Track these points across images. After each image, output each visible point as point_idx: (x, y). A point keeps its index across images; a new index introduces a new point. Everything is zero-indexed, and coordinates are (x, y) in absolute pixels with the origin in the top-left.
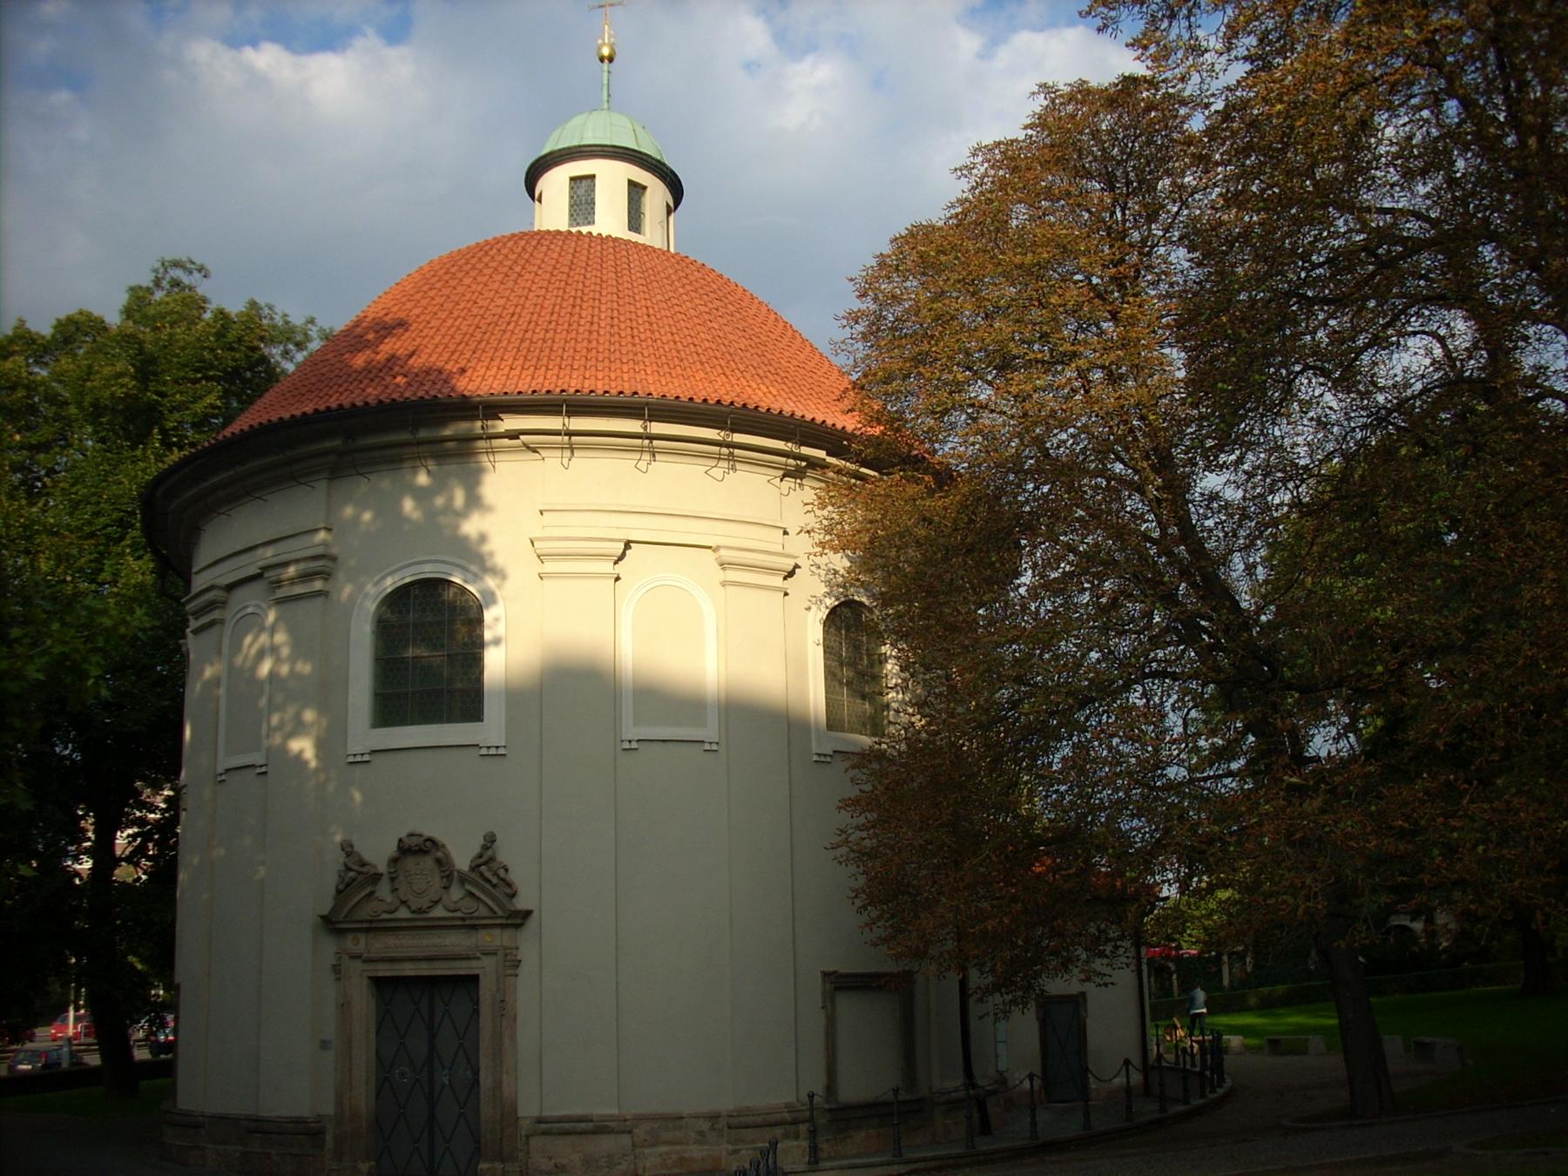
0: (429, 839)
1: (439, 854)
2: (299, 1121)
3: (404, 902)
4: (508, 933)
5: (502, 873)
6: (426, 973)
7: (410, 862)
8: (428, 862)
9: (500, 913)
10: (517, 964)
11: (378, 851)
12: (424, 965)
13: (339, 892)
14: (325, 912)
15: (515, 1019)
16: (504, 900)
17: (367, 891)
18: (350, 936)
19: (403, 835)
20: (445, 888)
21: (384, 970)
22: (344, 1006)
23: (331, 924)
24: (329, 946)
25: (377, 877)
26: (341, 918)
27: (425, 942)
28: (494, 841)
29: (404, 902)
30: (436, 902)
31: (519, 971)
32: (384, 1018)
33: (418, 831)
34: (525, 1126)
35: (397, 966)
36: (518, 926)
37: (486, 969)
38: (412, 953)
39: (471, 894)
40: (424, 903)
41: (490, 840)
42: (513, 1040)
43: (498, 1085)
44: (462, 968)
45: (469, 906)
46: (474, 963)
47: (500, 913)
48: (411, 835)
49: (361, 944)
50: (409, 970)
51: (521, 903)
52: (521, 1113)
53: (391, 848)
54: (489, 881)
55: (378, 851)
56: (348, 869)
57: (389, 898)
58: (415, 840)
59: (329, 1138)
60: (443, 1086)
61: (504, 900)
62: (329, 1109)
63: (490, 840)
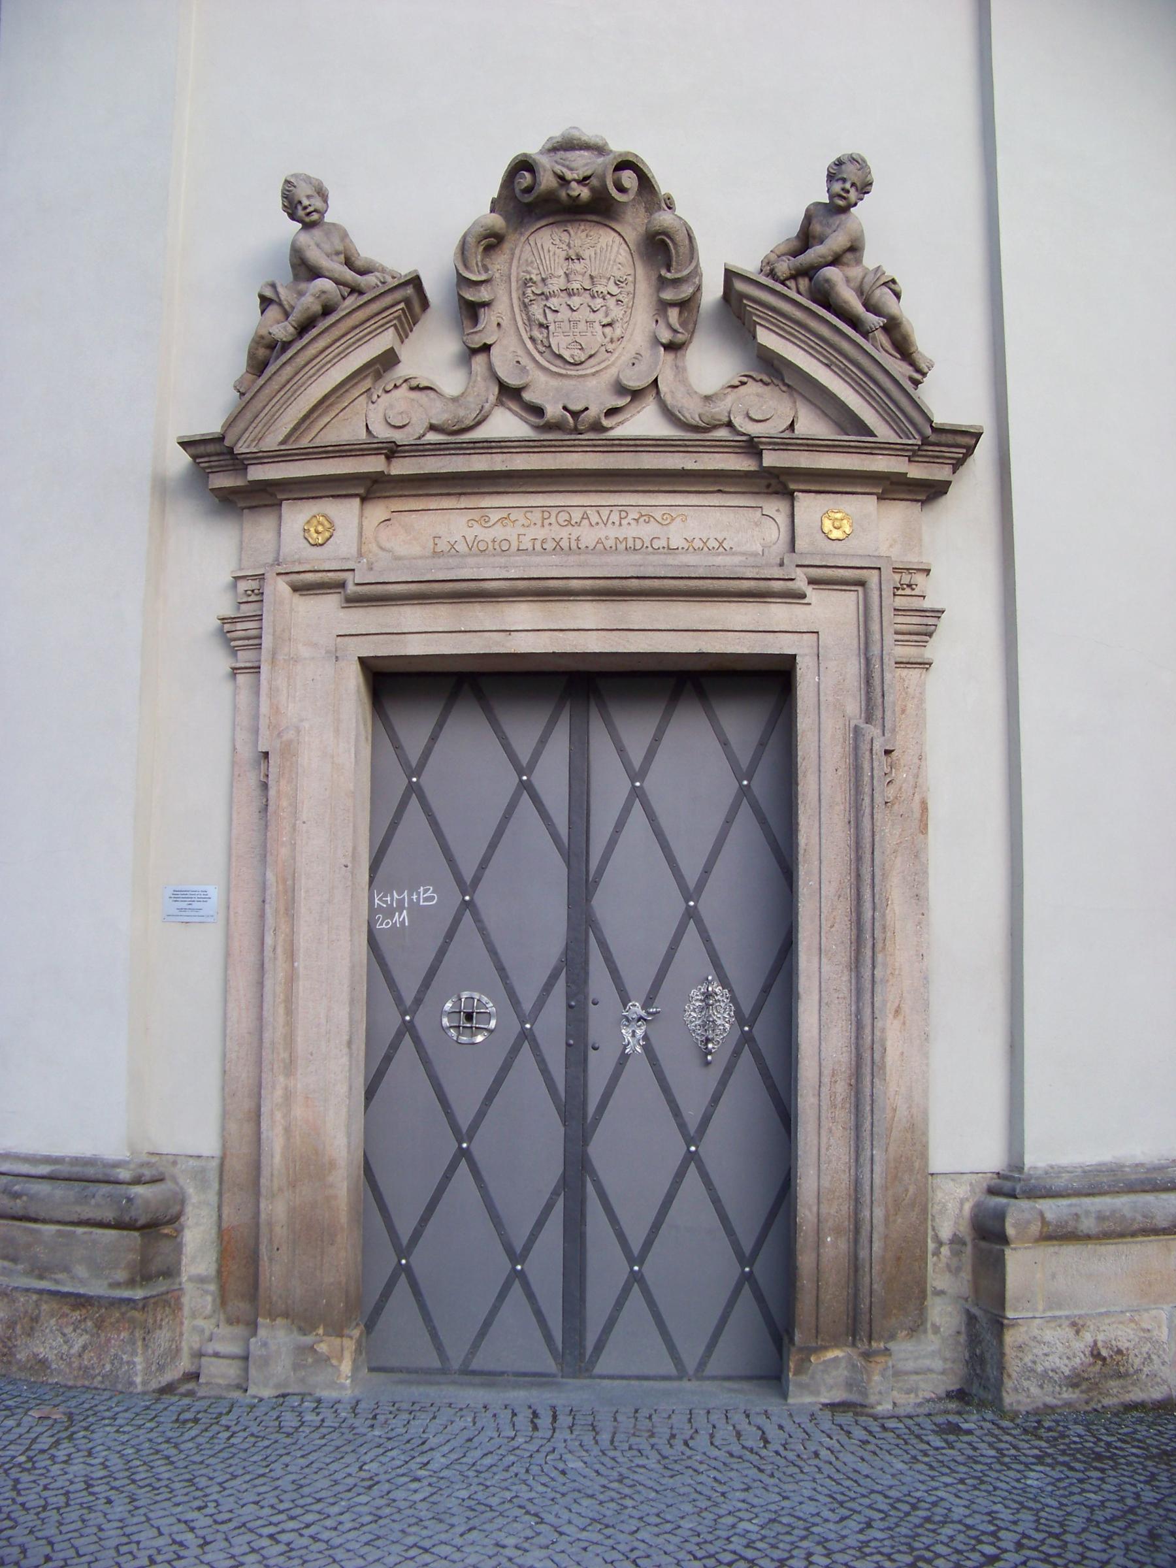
0: (626, 164)
1: (664, 218)
2: (83, 1176)
3: (509, 393)
4: (899, 513)
5: (884, 296)
6: (594, 644)
7: (546, 249)
8: (609, 251)
9: (883, 432)
10: (925, 624)
11: (415, 212)
12: (588, 614)
13: (258, 366)
14: (212, 425)
15: (923, 828)
16: (908, 386)
17: (385, 340)
18: (297, 518)
19: (532, 146)
20: (672, 347)
21: (425, 634)
22: (263, 768)
23: (229, 477)
24: (210, 556)
25: (411, 297)
26: (271, 442)
27: (589, 536)
28: (864, 188)
29: (509, 393)
30: (636, 395)
31: (934, 650)
32: (399, 814)
33: (590, 132)
34: (952, 1208)
35: (480, 616)
36: (931, 492)
37: (815, 632)
38: (540, 570)
39: (772, 369)
40: (593, 395)
41: (848, 183)
42: (919, 897)
43: (864, 1064)
44: (732, 630)
45: (767, 411)
46: (778, 614)
47: (883, 432)
48: (567, 145)
49: (344, 533)
50: (526, 632)
51: (950, 399)
52: (939, 1161)
53: (475, 200)
54: (854, 322)
55: (415, 212)
56: (304, 269)
57: (451, 382)
58: (582, 163)
59: (197, 1248)
60: (624, 1058)
61: (908, 386)
62: (187, 1128)
63: (848, 183)
